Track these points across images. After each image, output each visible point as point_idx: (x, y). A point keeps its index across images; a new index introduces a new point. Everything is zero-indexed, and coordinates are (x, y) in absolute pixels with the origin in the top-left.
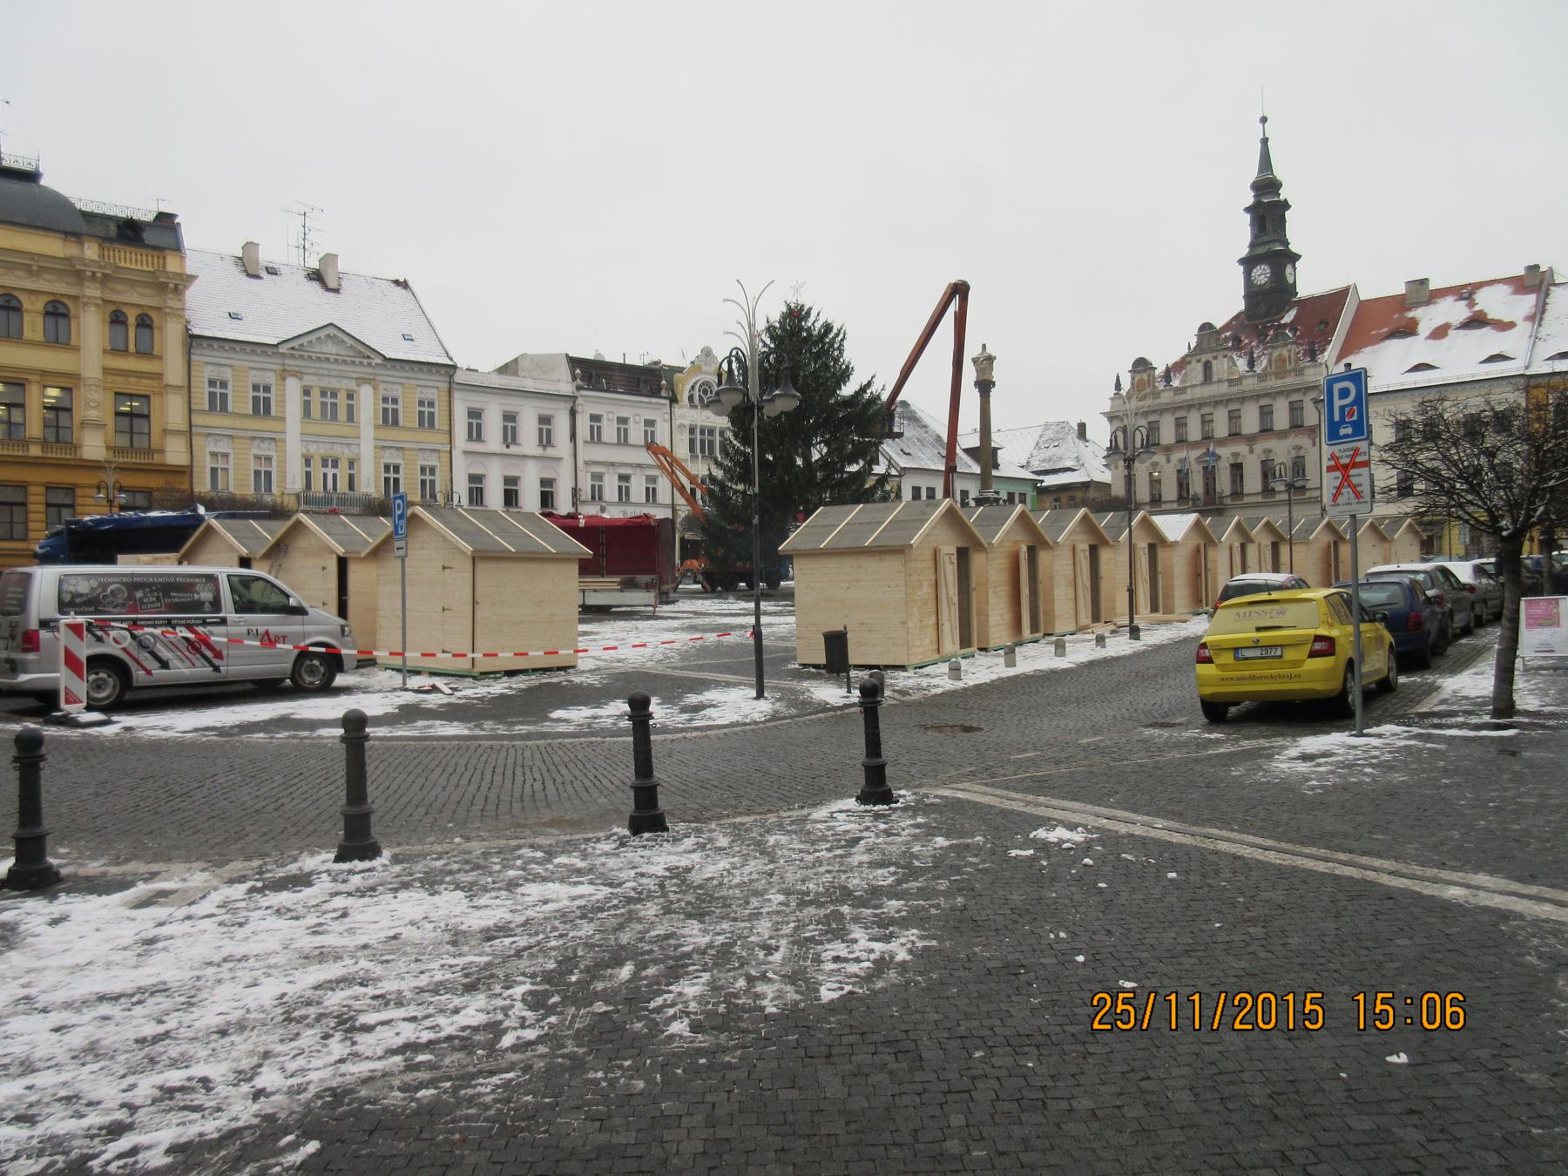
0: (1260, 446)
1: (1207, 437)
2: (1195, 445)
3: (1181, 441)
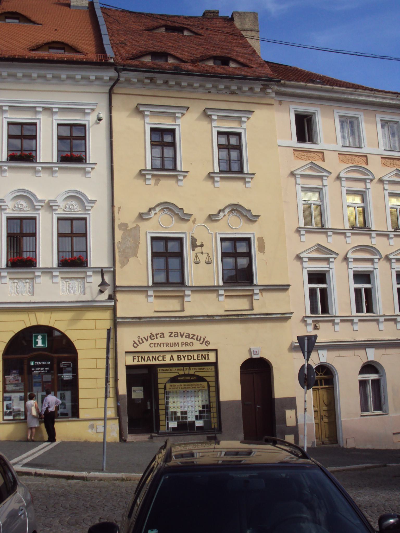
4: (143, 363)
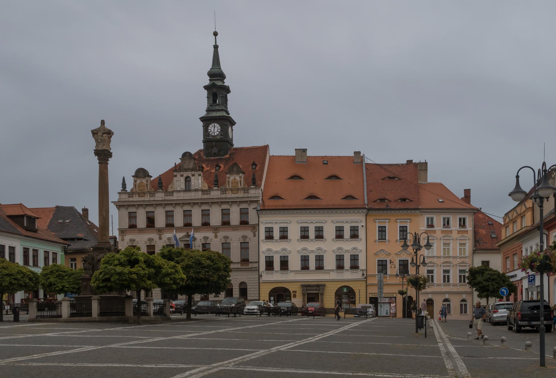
0: (221, 234)
1: (188, 225)
2: (179, 229)
3: (170, 226)
4: (375, 296)
